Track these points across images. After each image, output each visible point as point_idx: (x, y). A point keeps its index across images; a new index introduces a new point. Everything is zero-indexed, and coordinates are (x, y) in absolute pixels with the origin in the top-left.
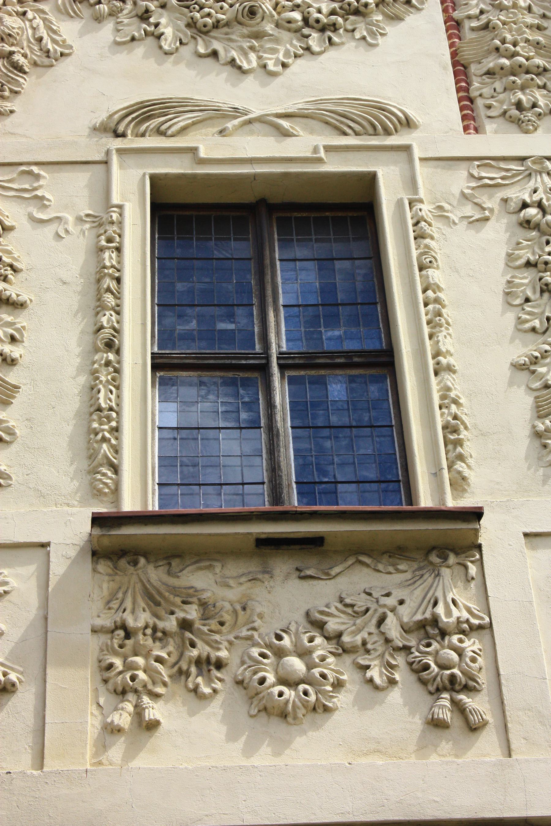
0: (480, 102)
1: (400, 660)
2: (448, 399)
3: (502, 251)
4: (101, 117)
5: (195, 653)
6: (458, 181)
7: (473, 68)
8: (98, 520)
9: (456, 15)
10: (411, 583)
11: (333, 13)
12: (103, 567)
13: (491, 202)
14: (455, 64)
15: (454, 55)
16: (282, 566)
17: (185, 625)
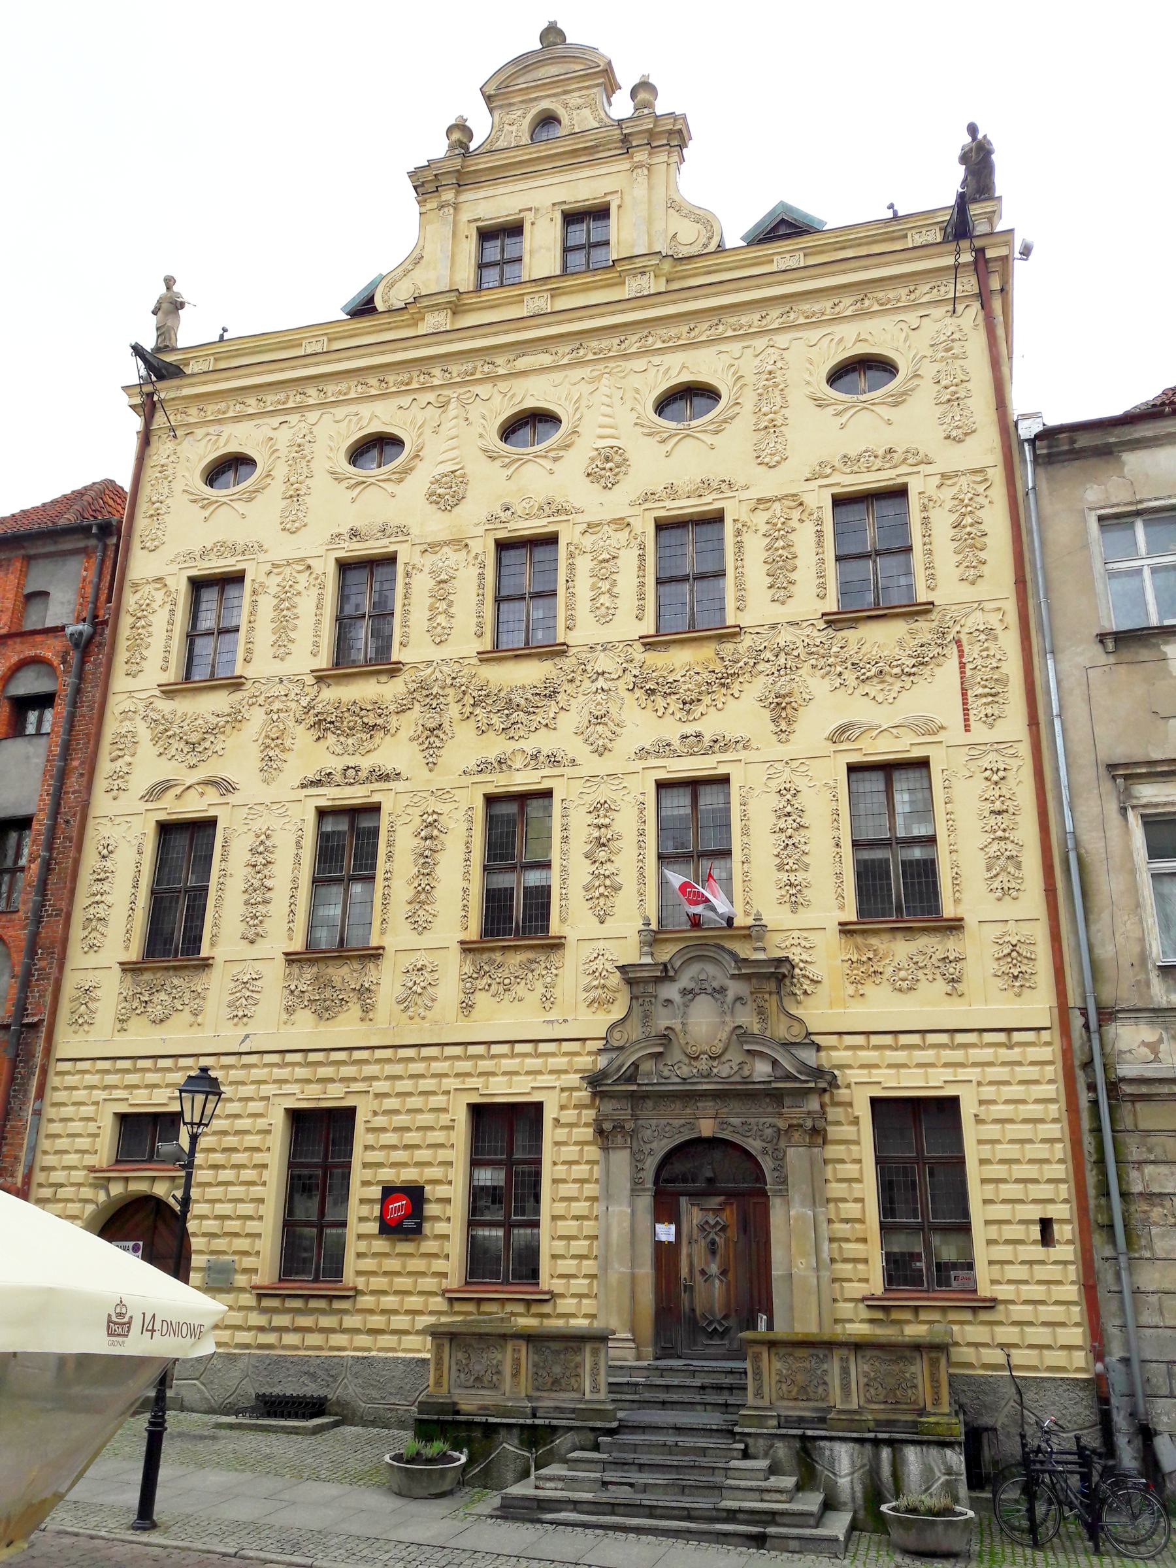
0: (971, 712)
1: (937, 971)
2: (955, 865)
3: (979, 792)
4: (827, 734)
5: (872, 969)
6: (962, 755)
7: (970, 693)
8: (840, 924)
9: (964, 660)
10: (939, 943)
11: (914, 666)
12: (843, 936)
13: (973, 765)
14: (963, 689)
15: (962, 683)
16: (899, 935)
17: (870, 959)
